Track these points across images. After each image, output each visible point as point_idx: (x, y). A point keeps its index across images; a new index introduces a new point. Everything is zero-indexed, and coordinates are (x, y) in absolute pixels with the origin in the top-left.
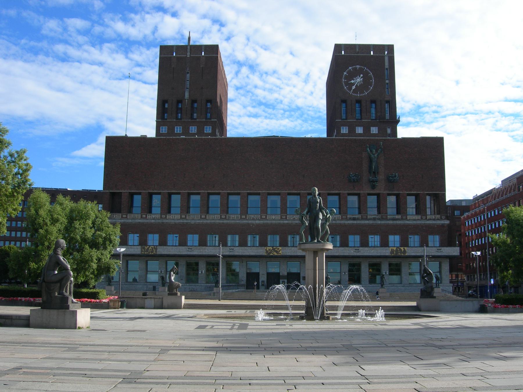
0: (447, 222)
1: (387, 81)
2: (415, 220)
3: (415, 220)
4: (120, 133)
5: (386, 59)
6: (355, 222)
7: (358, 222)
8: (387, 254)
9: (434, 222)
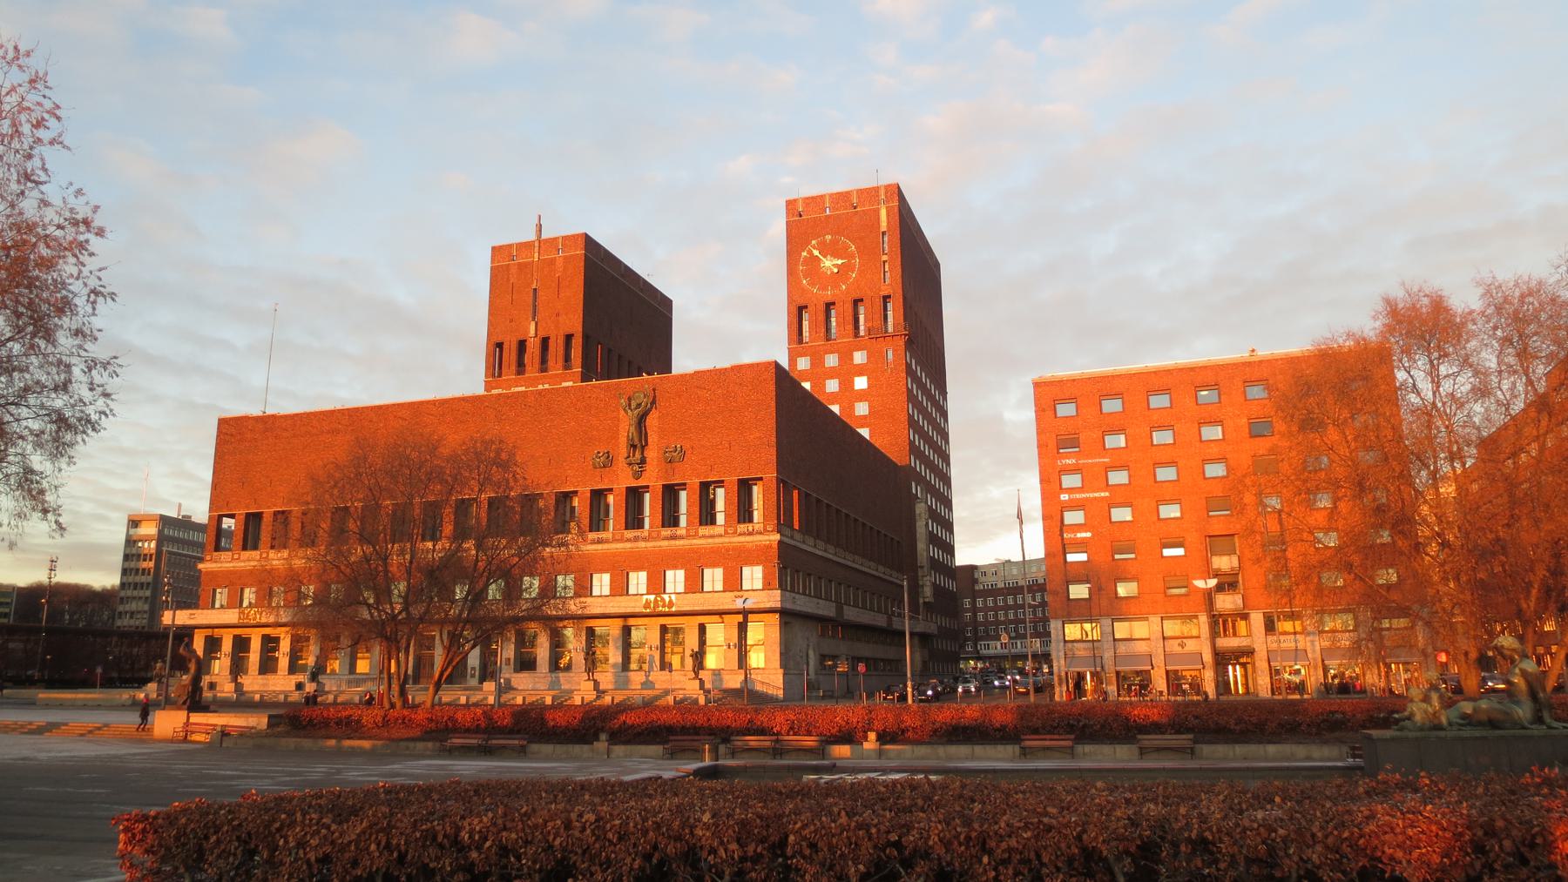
0: (777, 537)
1: (885, 258)
2: (712, 537)
3: (712, 537)
4: (251, 409)
5: (883, 213)
6: (599, 547)
7: (606, 546)
8: (637, 610)
9: (748, 538)
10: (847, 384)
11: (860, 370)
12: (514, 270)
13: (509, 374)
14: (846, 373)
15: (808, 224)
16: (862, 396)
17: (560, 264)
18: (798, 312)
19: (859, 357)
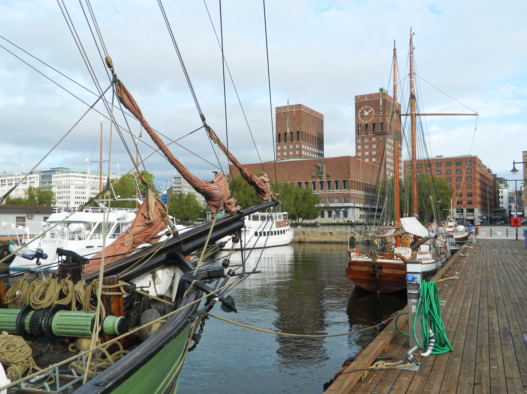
10: (370, 147)
11: (374, 143)
12: (282, 114)
13: (282, 143)
14: (370, 144)
15: (361, 103)
16: (374, 150)
17: (294, 112)
18: (358, 126)
19: (374, 139)
